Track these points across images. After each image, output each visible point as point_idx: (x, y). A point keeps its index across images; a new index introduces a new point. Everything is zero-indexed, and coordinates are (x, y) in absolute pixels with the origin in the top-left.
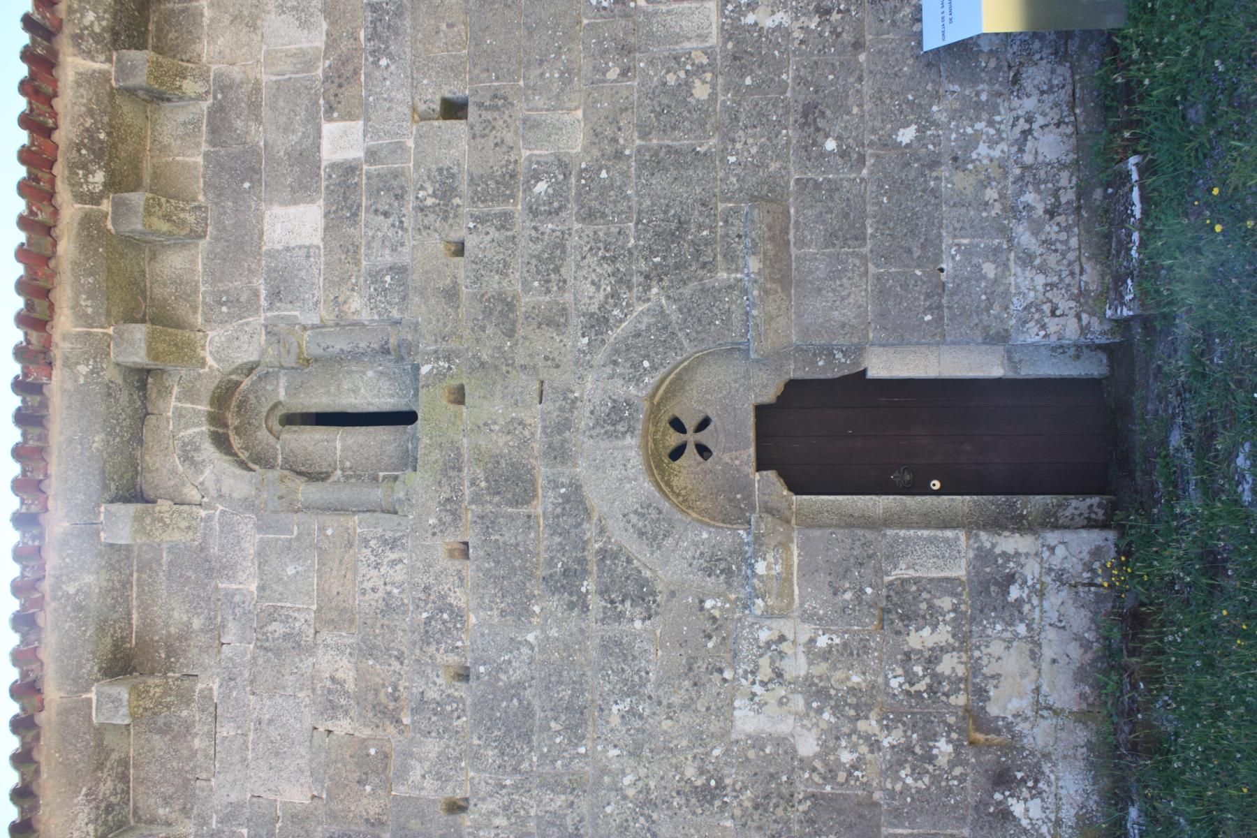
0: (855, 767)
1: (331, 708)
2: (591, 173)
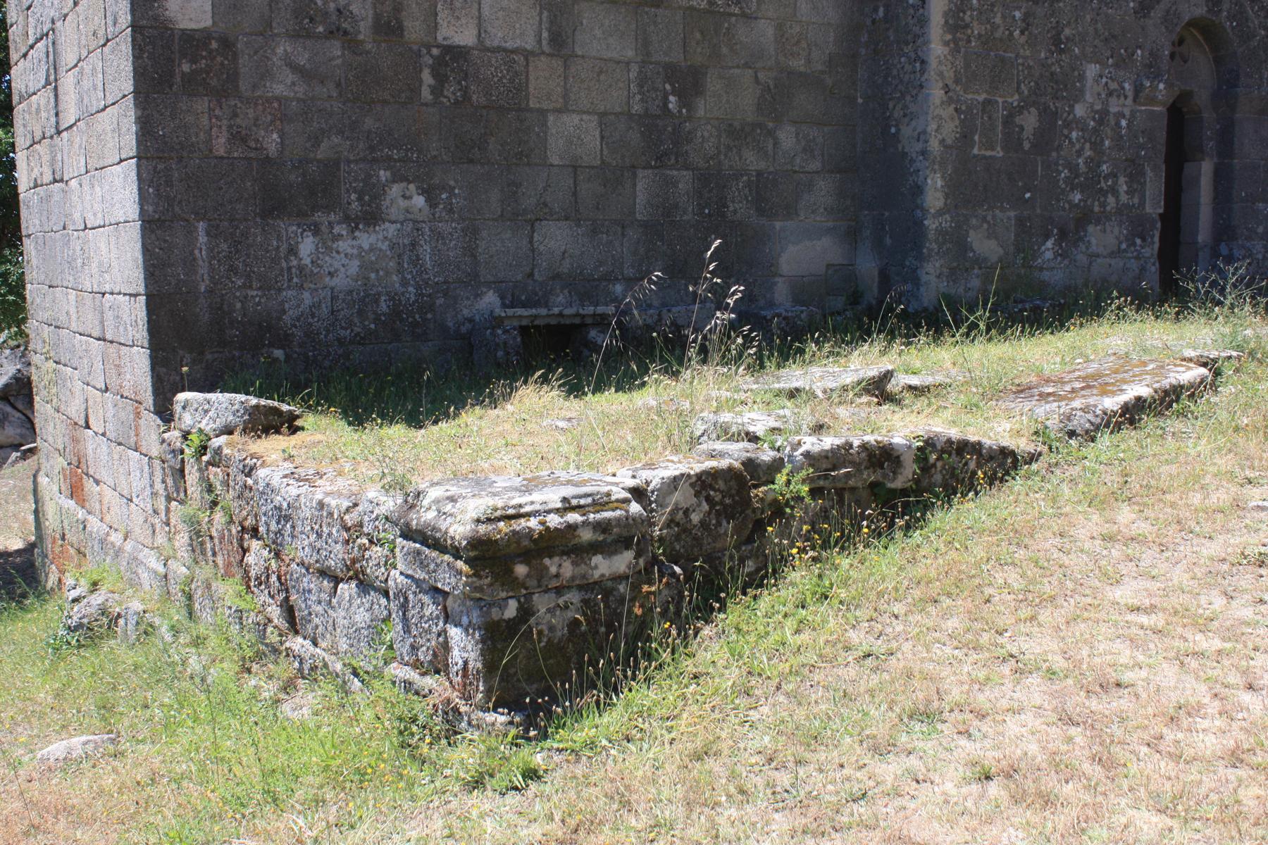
0: (1070, 139)
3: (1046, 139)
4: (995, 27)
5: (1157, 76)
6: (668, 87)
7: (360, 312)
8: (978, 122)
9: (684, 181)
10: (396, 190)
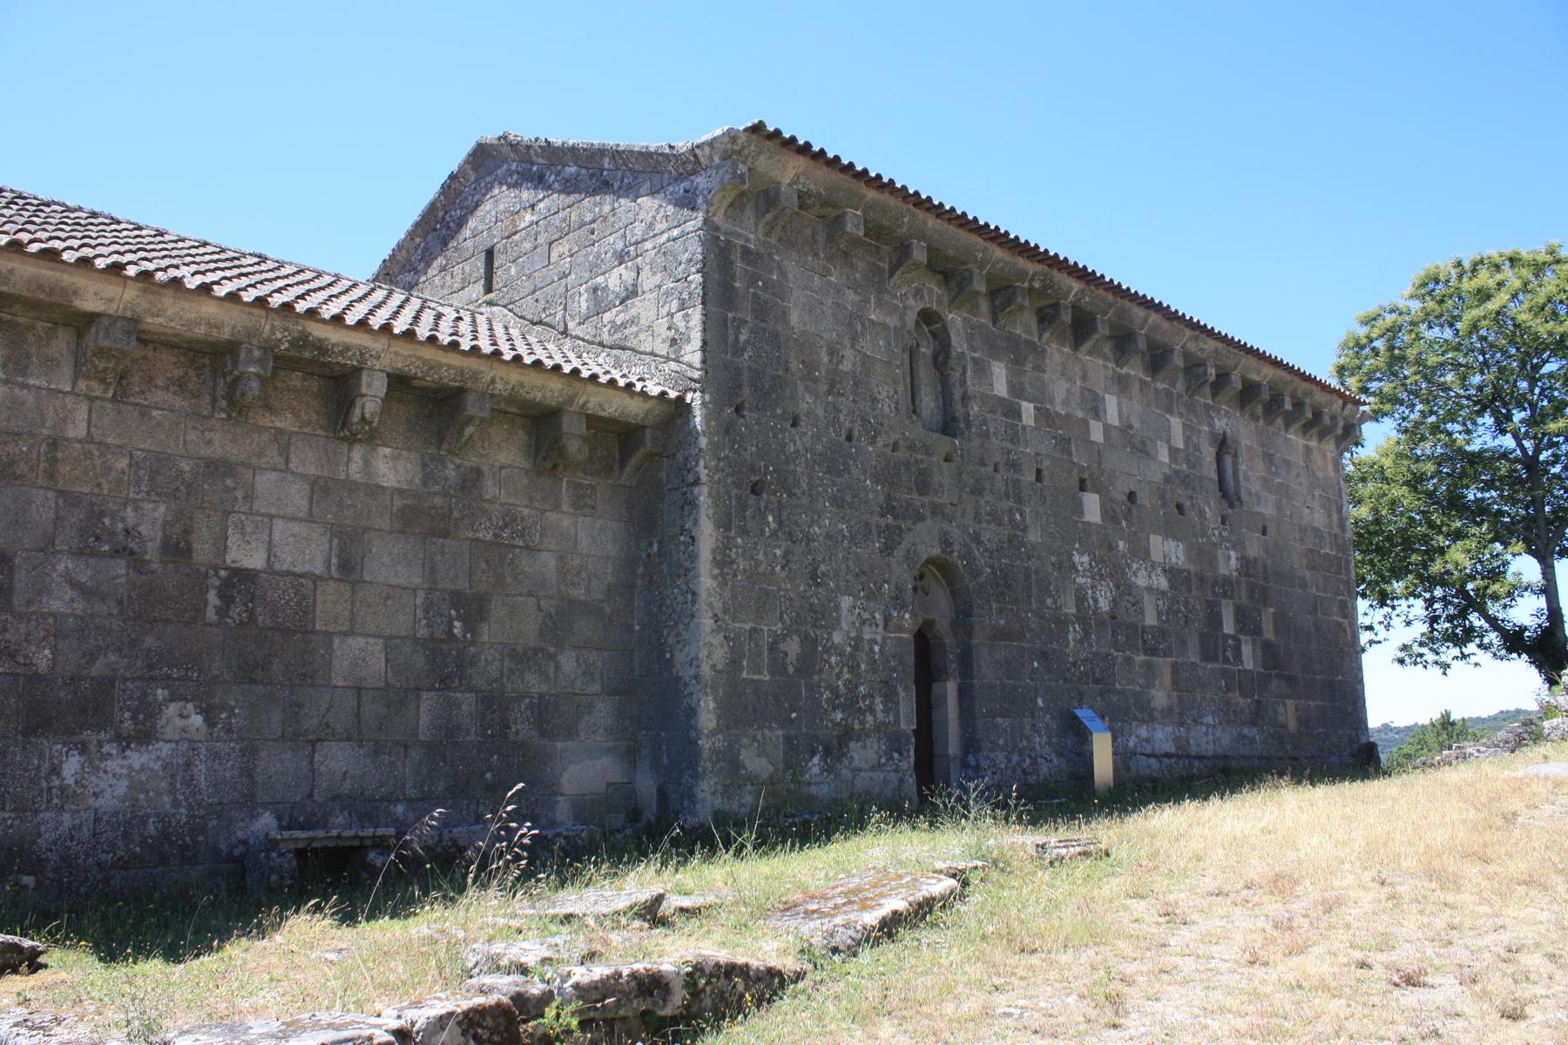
1: (832, 353)
2: (1023, 544)
3: (809, 663)
4: (758, 563)
5: (903, 607)
6: (453, 613)
7: (126, 835)
8: (746, 649)
9: (467, 703)
10: (173, 708)
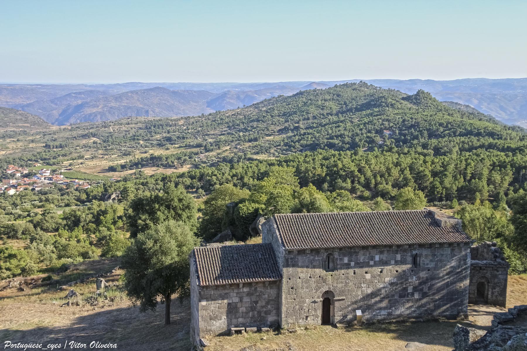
9: (256, 312)
